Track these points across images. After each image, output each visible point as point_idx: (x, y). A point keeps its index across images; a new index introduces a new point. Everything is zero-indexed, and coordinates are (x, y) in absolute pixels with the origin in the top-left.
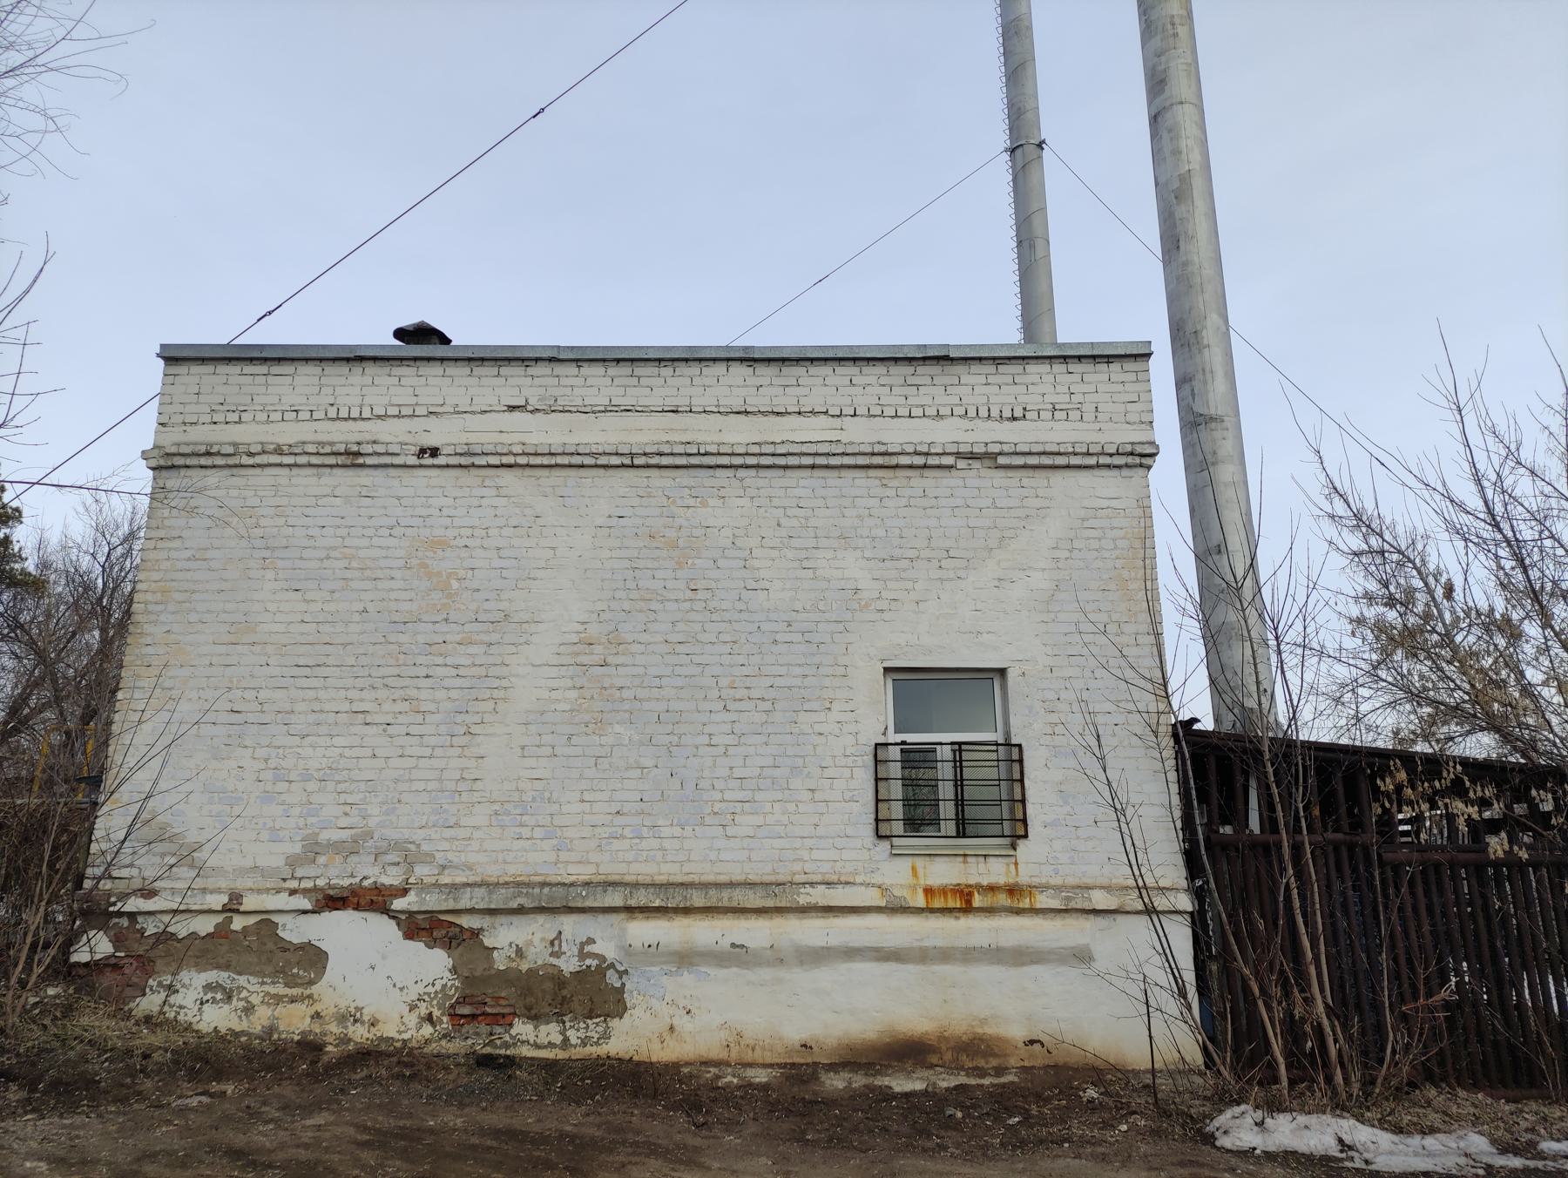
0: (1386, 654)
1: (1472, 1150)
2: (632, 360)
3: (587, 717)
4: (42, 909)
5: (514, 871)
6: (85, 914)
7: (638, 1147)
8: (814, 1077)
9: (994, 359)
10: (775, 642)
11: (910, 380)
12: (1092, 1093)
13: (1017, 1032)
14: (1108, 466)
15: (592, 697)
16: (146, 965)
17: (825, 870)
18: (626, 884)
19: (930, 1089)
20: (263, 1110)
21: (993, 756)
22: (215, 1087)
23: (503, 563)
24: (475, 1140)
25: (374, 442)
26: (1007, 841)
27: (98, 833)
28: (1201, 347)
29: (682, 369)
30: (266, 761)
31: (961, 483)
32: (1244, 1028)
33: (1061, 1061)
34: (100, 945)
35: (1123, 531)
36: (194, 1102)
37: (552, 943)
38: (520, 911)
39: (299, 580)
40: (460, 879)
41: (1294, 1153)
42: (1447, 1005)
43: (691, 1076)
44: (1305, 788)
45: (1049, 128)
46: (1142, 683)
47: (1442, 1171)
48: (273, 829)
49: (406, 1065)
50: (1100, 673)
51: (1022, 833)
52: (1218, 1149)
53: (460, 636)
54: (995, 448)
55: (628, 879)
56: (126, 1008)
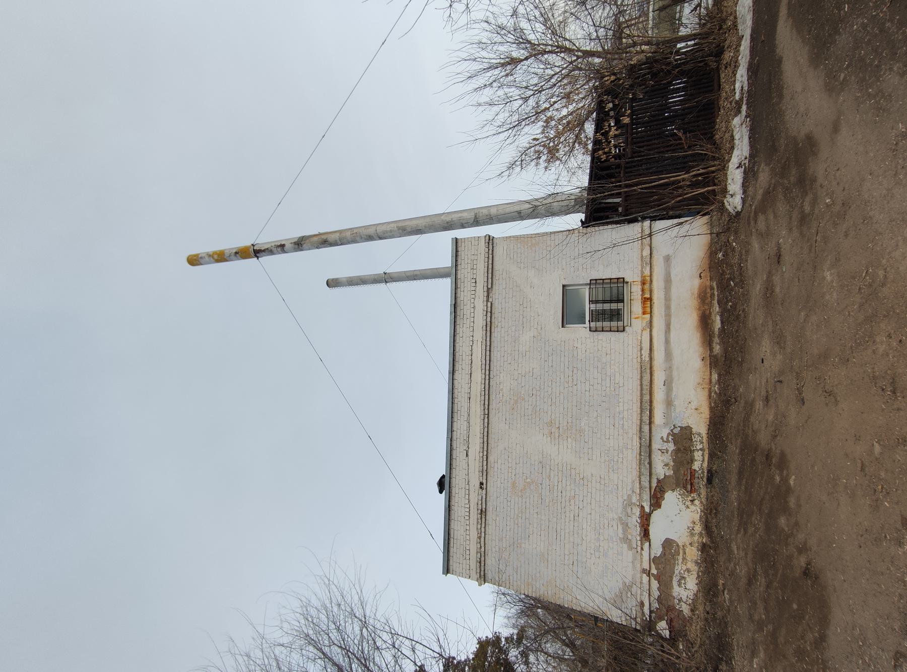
0: (558, 159)
1: (740, 123)
2: (452, 412)
3: (578, 436)
4: (648, 646)
5: (635, 465)
6: (650, 631)
7: (745, 425)
8: (715, 356)
9: (455, 289)
10: (552, 366)
11: (462, 317)
12: (720, 255)
13: (697, 282)
14: (493, 251)
15: (571, 433)
16: (670, 609)
17: (636, 350)
18: (641, 424)
19: (720, 314)
20: (730, 569)
21: (594, 290)
22: (720, 587)
23: (521, 462)
24: (743, 487)
25: (478, 504)
26: (625, 285)
27: (619, 621)
28: (452, 221)
29: (455, 395)
30: (591, 554)
31: (497, 300)
32: (694, 202)
33: (708, 266)
34: (662, 626)
35: (515, 245)
36: (727, 596)
37: (663, 453)
38: (650, 464)
39: (525, 535)
40: (638, 486)
41: (743, 183)
42: (685, 133)
43: (715, 403)
44: (606, 184)
45: (380, 271)
46: (568, 238)
47: (748, 133)
48: (618, 554)
49: (711, 511)
50: (564, 252)
51: (622, 279)
52: (742, 210)
53: (547, 479)
54: (485, 288)
55: (639, 423)
56: (688, 618)
